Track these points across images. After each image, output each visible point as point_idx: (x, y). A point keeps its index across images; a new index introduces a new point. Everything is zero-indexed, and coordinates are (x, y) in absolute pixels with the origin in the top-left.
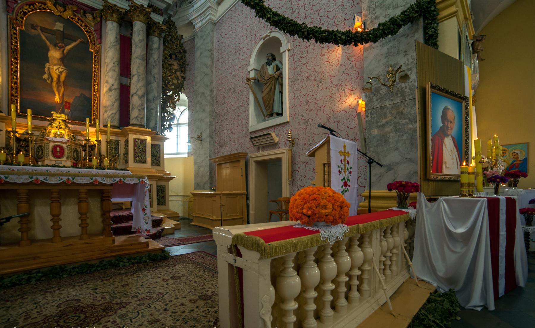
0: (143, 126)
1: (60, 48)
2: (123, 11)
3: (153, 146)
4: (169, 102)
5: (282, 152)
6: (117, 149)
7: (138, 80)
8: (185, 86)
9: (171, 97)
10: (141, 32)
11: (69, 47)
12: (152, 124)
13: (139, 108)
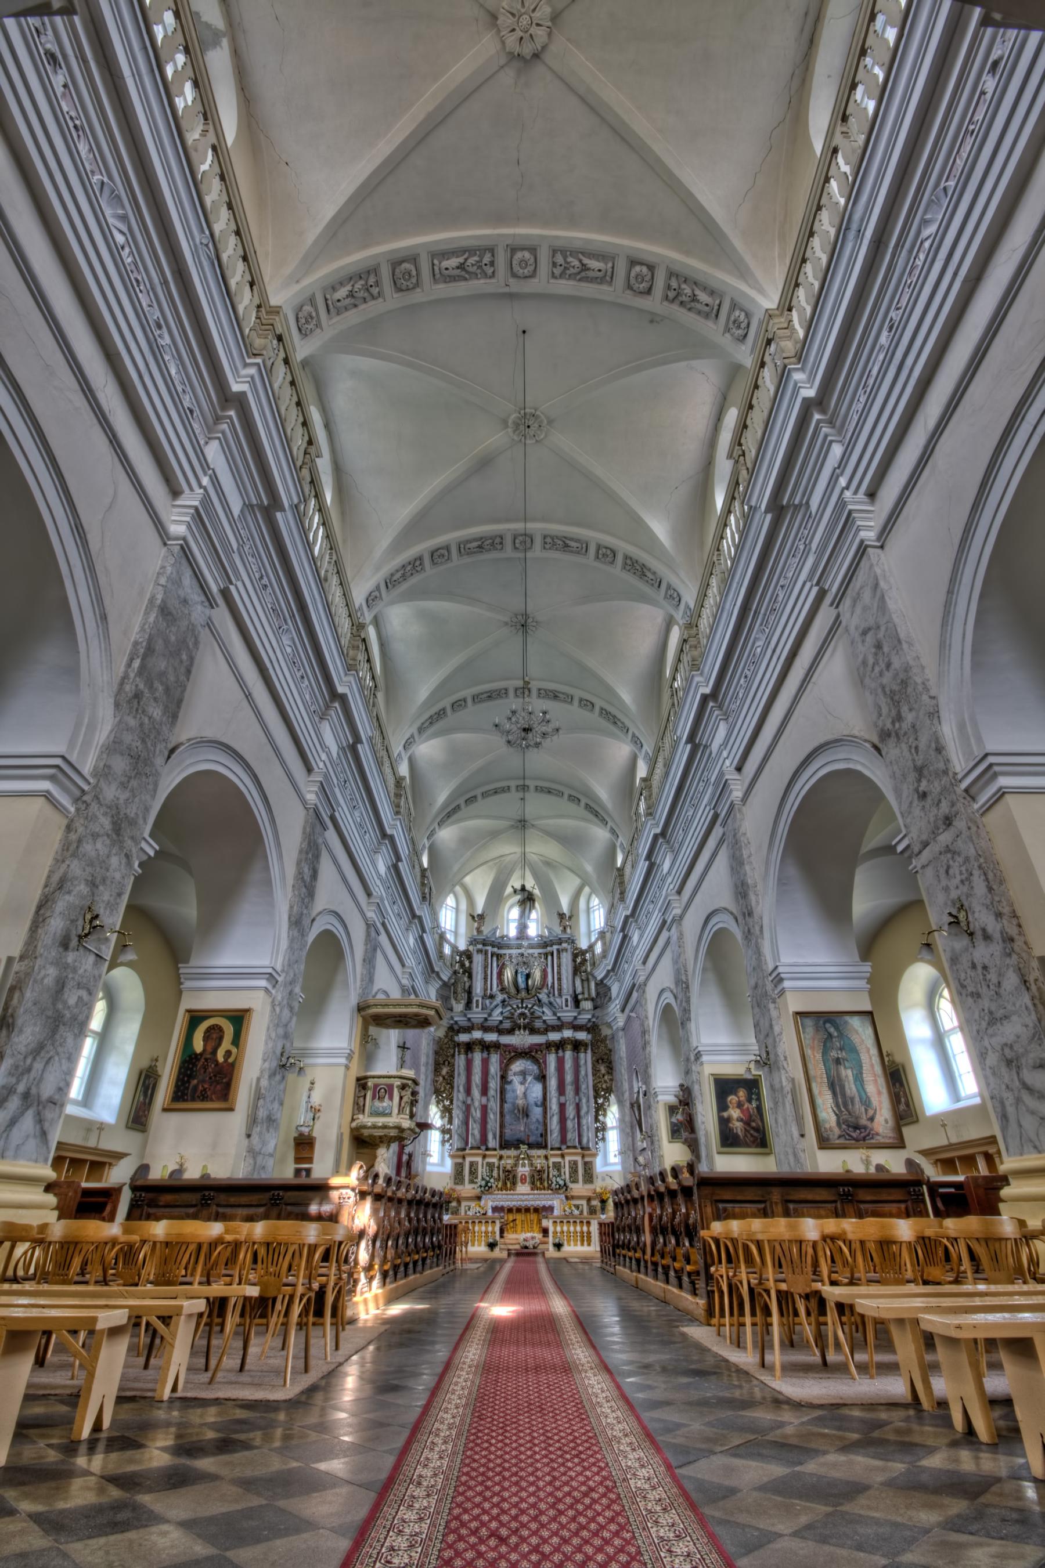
0: (575, 1147)
3: (586, 1164)
4: (600, 1110)
9: (603, 1104)
12: (585, 1140)
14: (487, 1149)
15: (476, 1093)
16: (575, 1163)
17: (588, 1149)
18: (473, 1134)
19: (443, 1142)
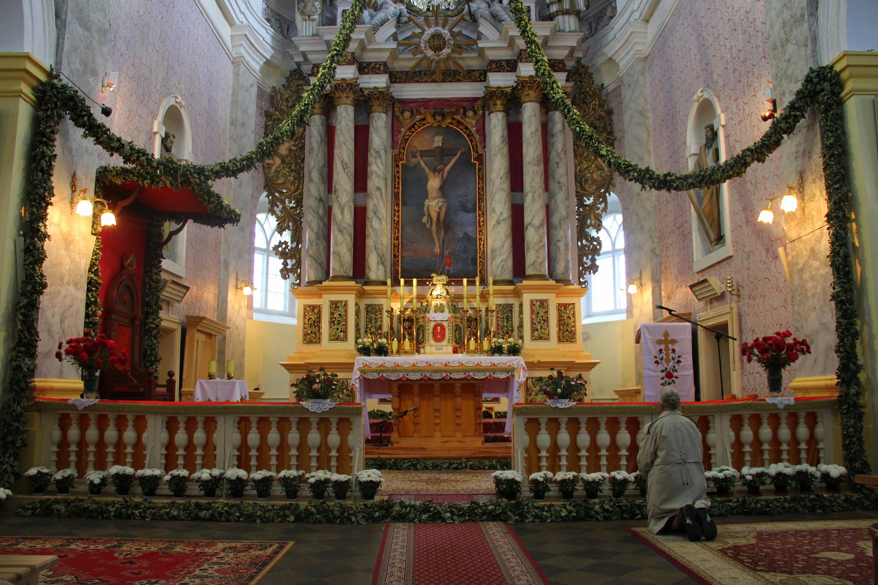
0: (541, 277)
1: (439, 172)
2: (509, 90)
6: (509, 319)
7: (533, 200)
9: (593, 207)
10: (533, 118)
11: (448, 167)
12: (560, 268)
13: (536, 248)
14: (368, 283)
15: (344, 181)
16: (543, 303)
17: (567, 282)
18: (338, 254)
19: (285, 273)
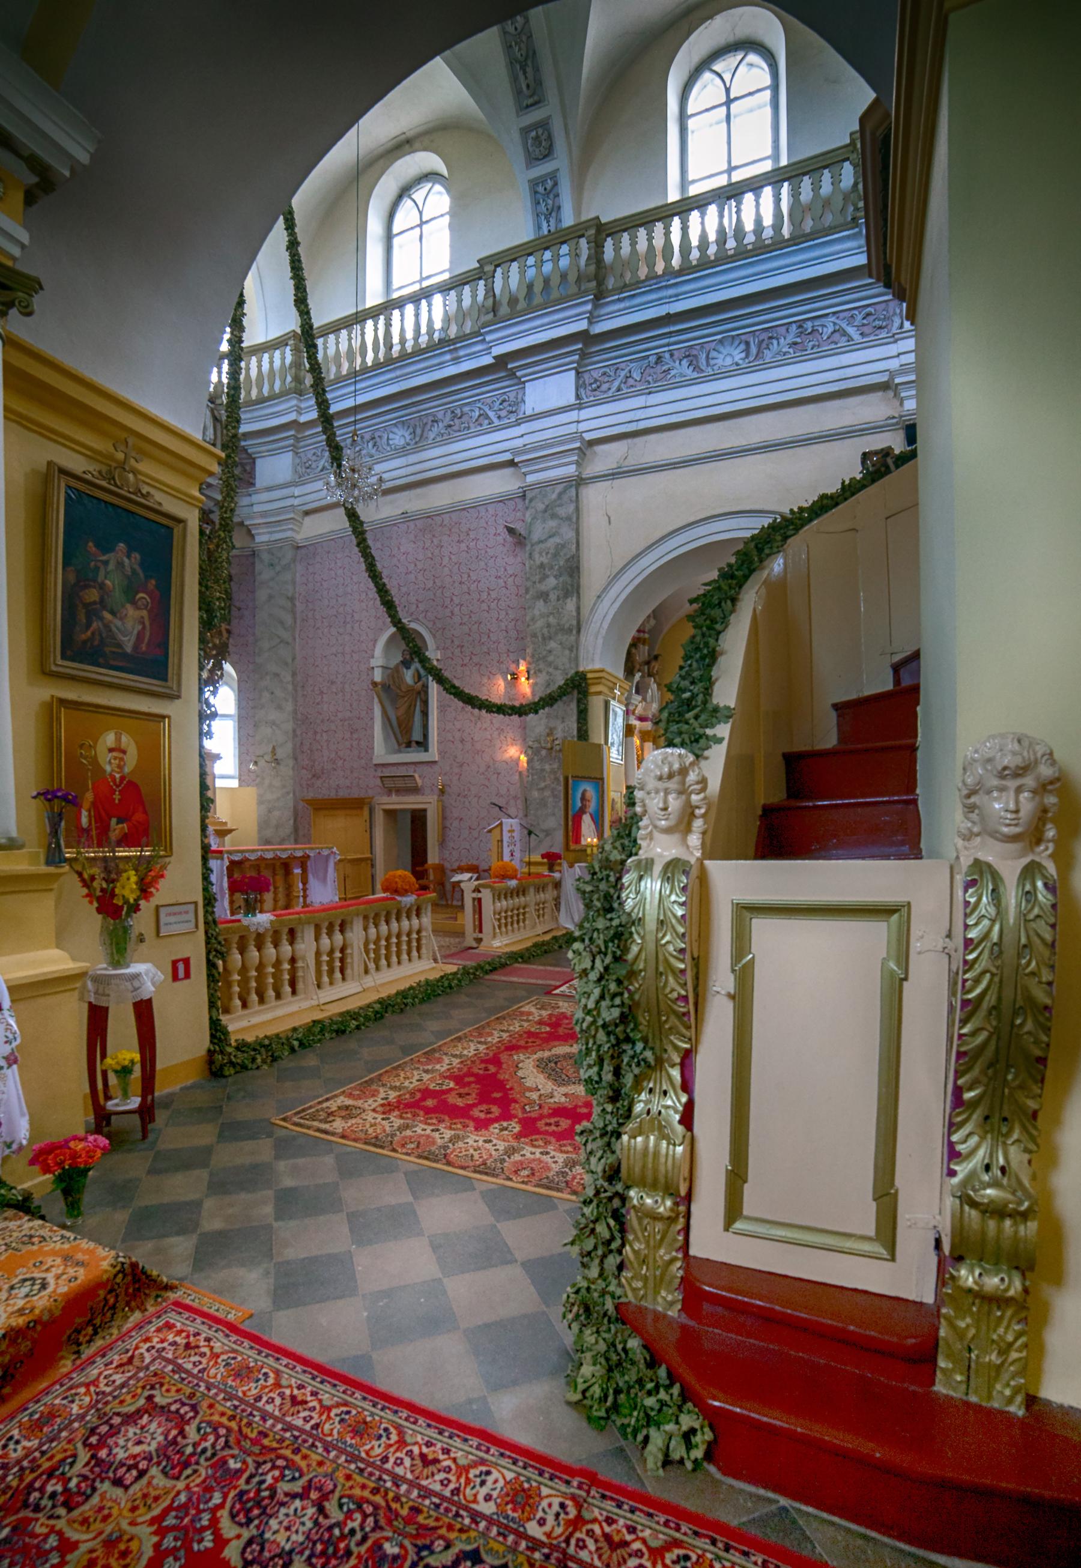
5: (428, 802)
8: (231, 649)
